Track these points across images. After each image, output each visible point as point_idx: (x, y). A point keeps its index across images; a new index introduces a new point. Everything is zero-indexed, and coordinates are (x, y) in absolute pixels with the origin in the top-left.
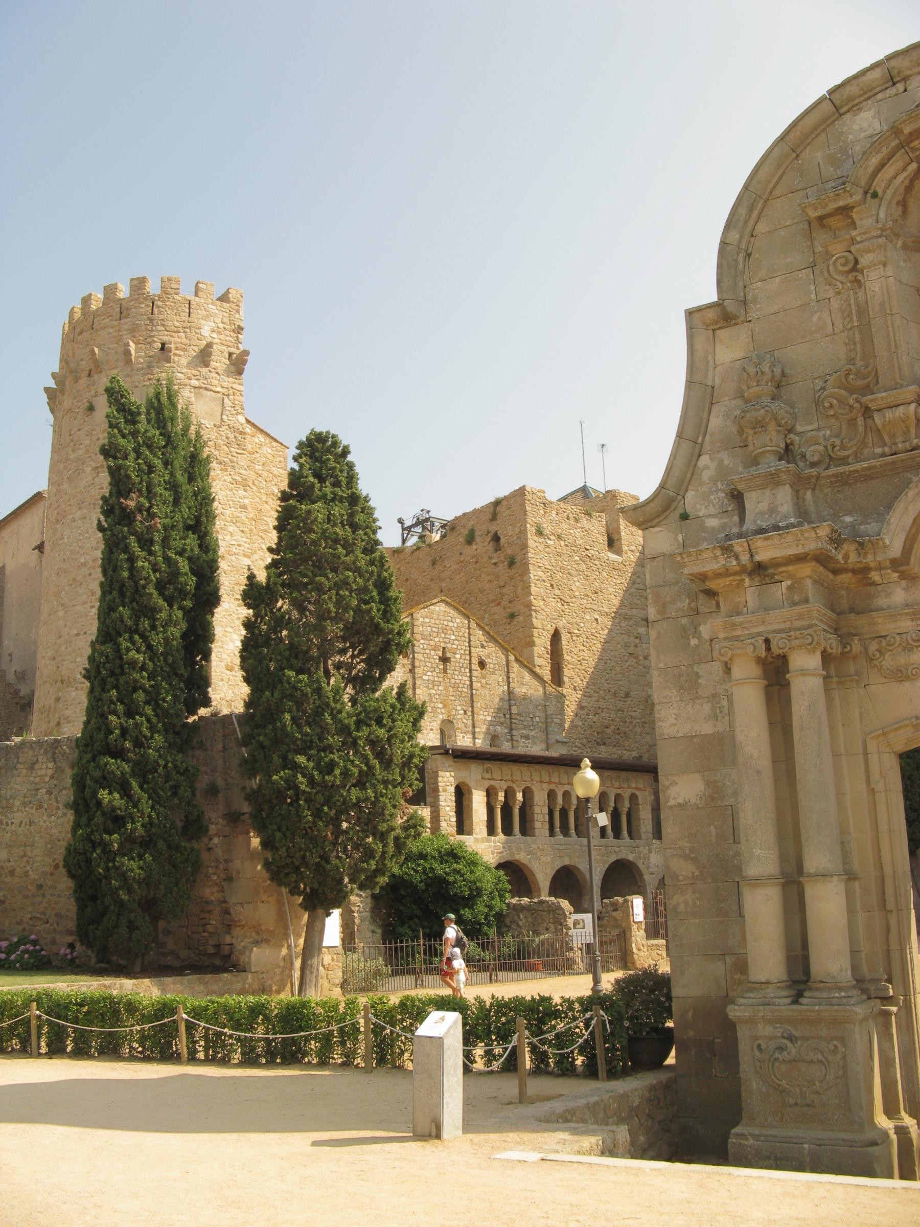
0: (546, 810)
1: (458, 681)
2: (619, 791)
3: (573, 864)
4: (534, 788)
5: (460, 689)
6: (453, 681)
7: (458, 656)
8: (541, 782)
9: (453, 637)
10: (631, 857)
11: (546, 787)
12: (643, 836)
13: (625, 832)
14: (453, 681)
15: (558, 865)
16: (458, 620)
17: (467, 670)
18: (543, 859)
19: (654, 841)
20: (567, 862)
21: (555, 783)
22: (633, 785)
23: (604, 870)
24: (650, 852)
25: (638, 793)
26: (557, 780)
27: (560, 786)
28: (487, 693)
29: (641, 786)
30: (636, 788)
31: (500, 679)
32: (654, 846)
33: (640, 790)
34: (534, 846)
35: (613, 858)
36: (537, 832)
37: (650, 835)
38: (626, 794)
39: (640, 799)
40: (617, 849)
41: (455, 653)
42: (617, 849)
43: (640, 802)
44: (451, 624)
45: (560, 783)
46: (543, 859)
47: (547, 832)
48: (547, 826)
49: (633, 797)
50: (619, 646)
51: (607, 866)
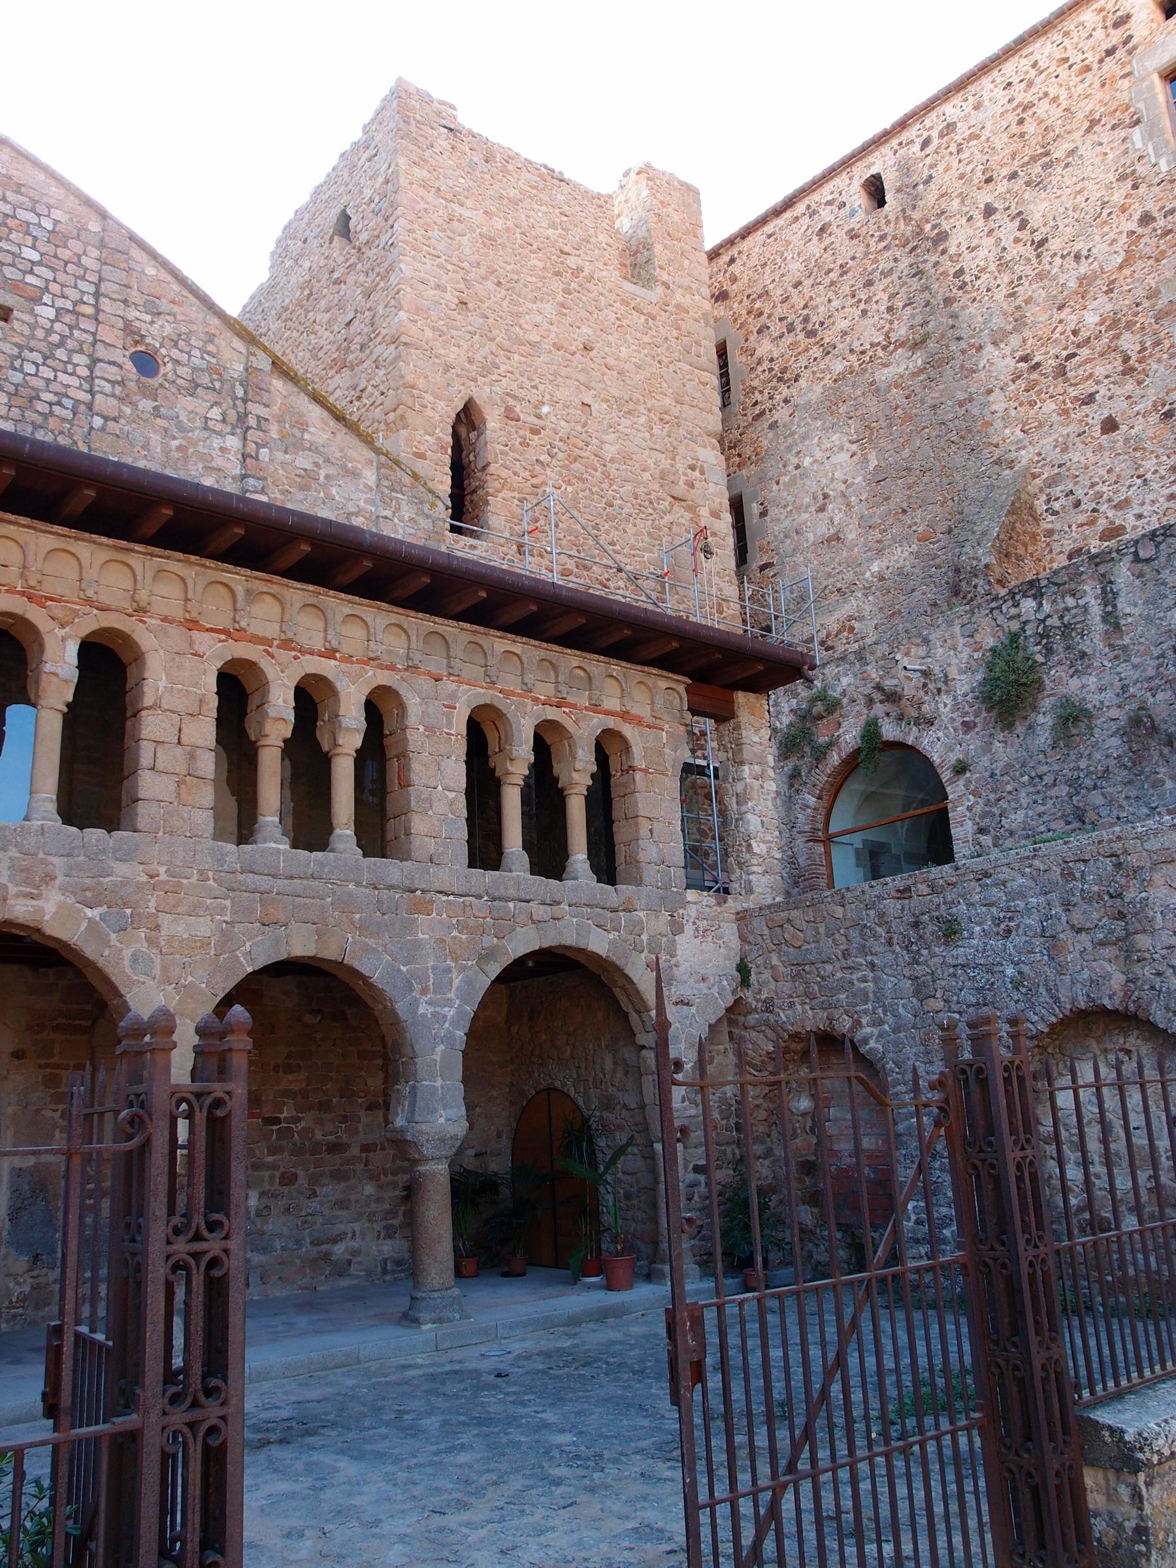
0: (204, 731)
1: (35, 382)
2: (552, 714)
3: (331, 954)
4: (145, 636)
5: (41, 407)
6: (17, 377)
7: (50, 313)
8: (192, 624)
9: (35, 256)
10: (599, 944)
11: (215, 653)
12: (650, 874)
13: (579, 857)
14: (17, 377)
15: (254, 953)
16: (57, 214)
17: (81, 359)
18: (173, 927)
19: (691, 895)
20: (301, 945)
21: (255, 639)
22: (612, 703)
23: (484, 982)
24: (677, 928)
25: (628, 731)
26: (271, 630)
27: (284, 655)
28: (155, 438)
29: (642, 710)
30: (625, 716)
31: (215, 413)
32: (692, 911)
33: (638, 721)
34: (121, 870)
35: (523, 942)
36: (145, 813)
37: (678, 875)
38: (584, 732)
39: (637, 750)
40: (540, 912)
41: (38, 301)
42: (540, 912)
43: (639, 761)
44: (32, 218)
45: (286, 644)
46: (173, 927)
47: (204, 820)
48: (207, 795)
49: (608, 748)
50: (647, 475)
51: (495, 969)
